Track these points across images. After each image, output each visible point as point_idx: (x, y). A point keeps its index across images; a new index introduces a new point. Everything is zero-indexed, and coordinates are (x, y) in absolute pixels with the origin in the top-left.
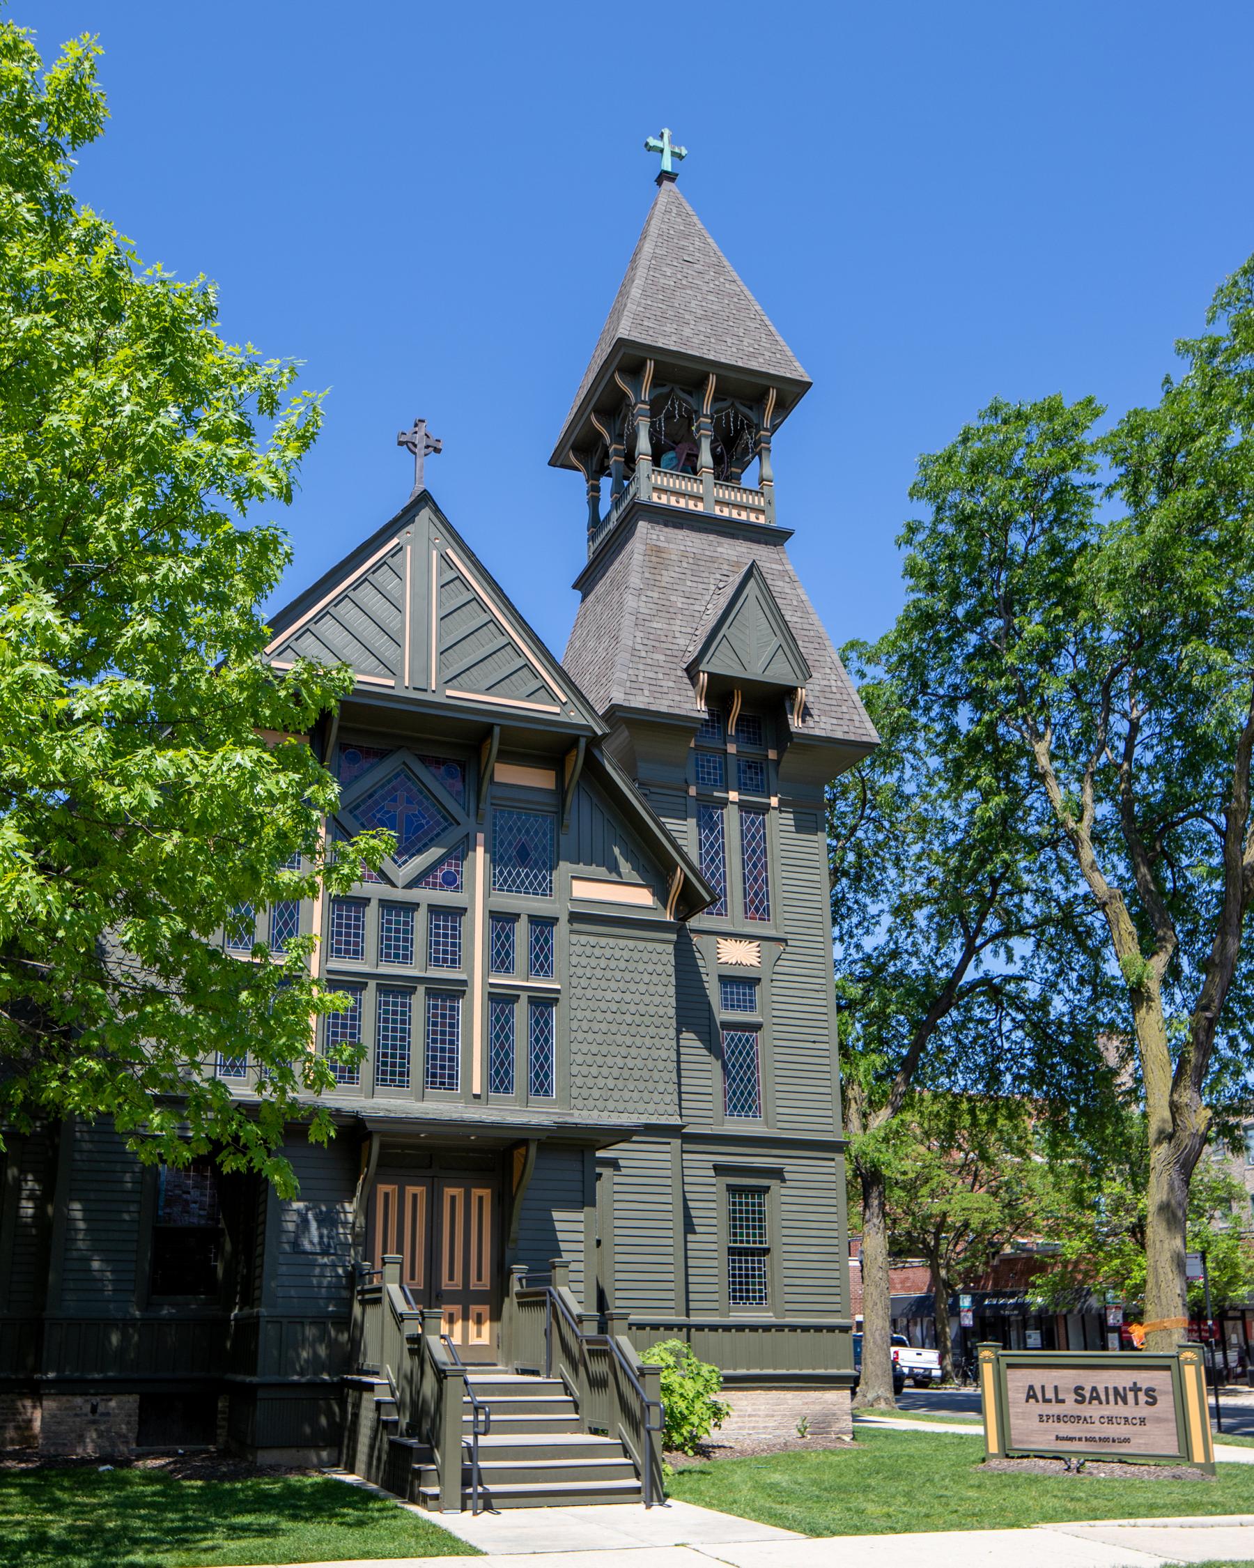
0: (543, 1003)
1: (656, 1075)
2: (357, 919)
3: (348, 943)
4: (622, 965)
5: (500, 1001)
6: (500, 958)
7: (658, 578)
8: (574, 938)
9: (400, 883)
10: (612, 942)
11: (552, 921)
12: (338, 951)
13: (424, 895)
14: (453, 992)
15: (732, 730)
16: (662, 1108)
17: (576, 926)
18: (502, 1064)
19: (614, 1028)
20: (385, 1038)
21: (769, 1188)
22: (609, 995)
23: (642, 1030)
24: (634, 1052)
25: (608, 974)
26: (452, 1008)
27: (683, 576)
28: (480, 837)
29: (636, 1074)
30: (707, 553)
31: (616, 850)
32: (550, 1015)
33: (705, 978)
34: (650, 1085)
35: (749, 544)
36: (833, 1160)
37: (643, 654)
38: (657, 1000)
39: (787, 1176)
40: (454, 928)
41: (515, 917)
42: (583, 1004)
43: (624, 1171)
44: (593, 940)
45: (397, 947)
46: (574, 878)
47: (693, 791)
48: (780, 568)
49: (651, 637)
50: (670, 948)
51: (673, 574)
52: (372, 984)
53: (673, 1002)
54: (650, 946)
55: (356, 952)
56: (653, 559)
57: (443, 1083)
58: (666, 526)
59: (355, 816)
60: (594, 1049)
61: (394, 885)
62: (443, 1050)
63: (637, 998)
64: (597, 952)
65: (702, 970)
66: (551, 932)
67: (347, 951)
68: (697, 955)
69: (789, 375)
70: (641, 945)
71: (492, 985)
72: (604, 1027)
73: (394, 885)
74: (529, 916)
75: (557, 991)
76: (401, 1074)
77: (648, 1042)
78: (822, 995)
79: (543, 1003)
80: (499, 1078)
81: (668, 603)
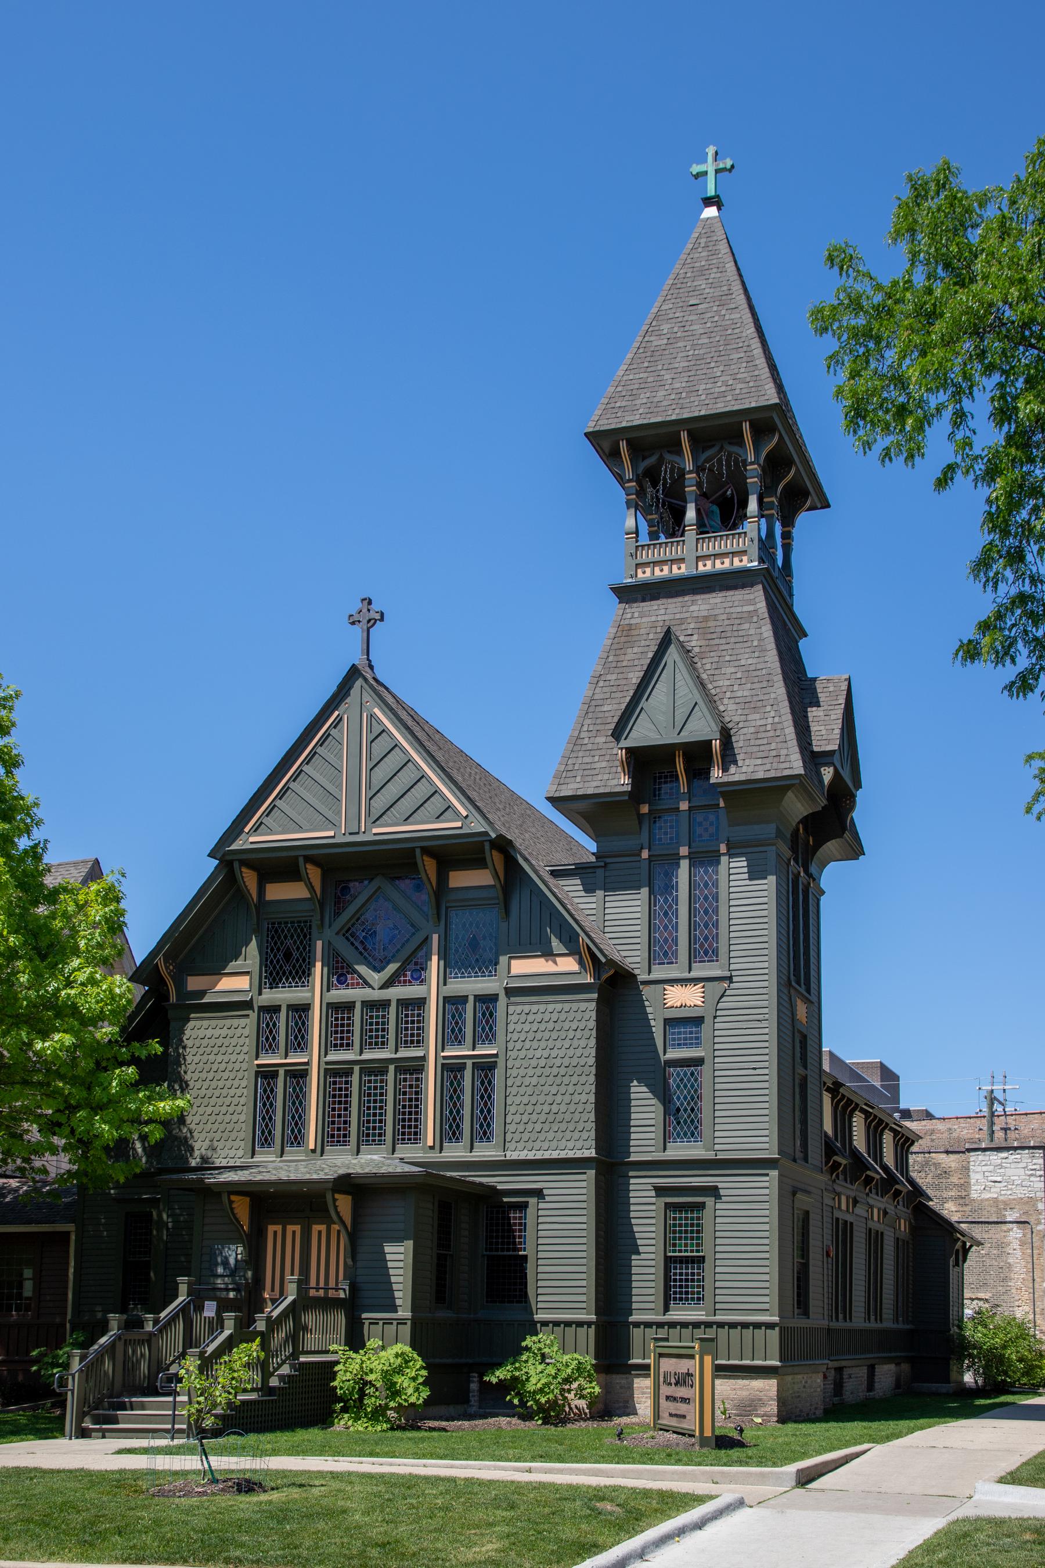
0: (486, 1068)
1: (577, 1116)
2: (349, 1018)
3: (342, 1038)
4: (550, 1026)
5: (451, 1070)
6: (451, 1034)
7: (622, 658)
8: (511, 1009)
9: (376, 986)
10: (542, 1008)
11: (493, 998)
12: (336, 1045)
13: (396, 993)
14: (416, 1067)
15: (683, 788)
16: (579, 1144)
17: (513, 999)
18: (454, 1119)
19: (542, 1081)
20: (369, 1108)
21: (705, 1203)
22: (538, 1054)
23: (566, 1080)
24: (559, 1098)
25: (539, 1035)
26: (417, 1079)
27: (646, 649)
28: (435, 937)
29: (560, 1117)
30: (678, 616)
31: (549, 930)
32: (493, 1076)
33: (652, 1023)
34: (571, 1127)
35: (724, 594)
36: (767, 1175)
37: (586, 741)
38: (579, 1052)
39: (722, 1192)
40: (419, 1015)
41: (464, 999)
42: (517, 1063)
43: (547, 1198)
44: (527, 1008)
45: (377, 1037)
46: (511, 958)
47: (645, 854)
48: (751, 608)
49: (599, 721)
50: (594, 1004)
51: (635, 650)
52: (357, 1069)
53: (593, 1052)
54: (575, 1006)
55: (348, 1045)
56: (623, 639)
57: (409, 1139)
58: (644, 601)
59: (347, 938)
60: (525, 1100)
61: (373, 989)
62: (410, 1113)
63: (561, 1053)
64: (531, 1018)
65: (650, 1017)
66: (495, 1007)
67: (342, 1045)
68: (646, 1003)
69: (753, 405)
70: (567, 1007)
71: (445, 1058)
72: (534, 1080)
73: (370, 986)
74: (475, 996)
75: (496, 1056)
76: (380, 1135)
77: (571, 1089)
78: (764, 1024)
79: (486, 1068)
80: (449, 1130)
81: (624, 682)
